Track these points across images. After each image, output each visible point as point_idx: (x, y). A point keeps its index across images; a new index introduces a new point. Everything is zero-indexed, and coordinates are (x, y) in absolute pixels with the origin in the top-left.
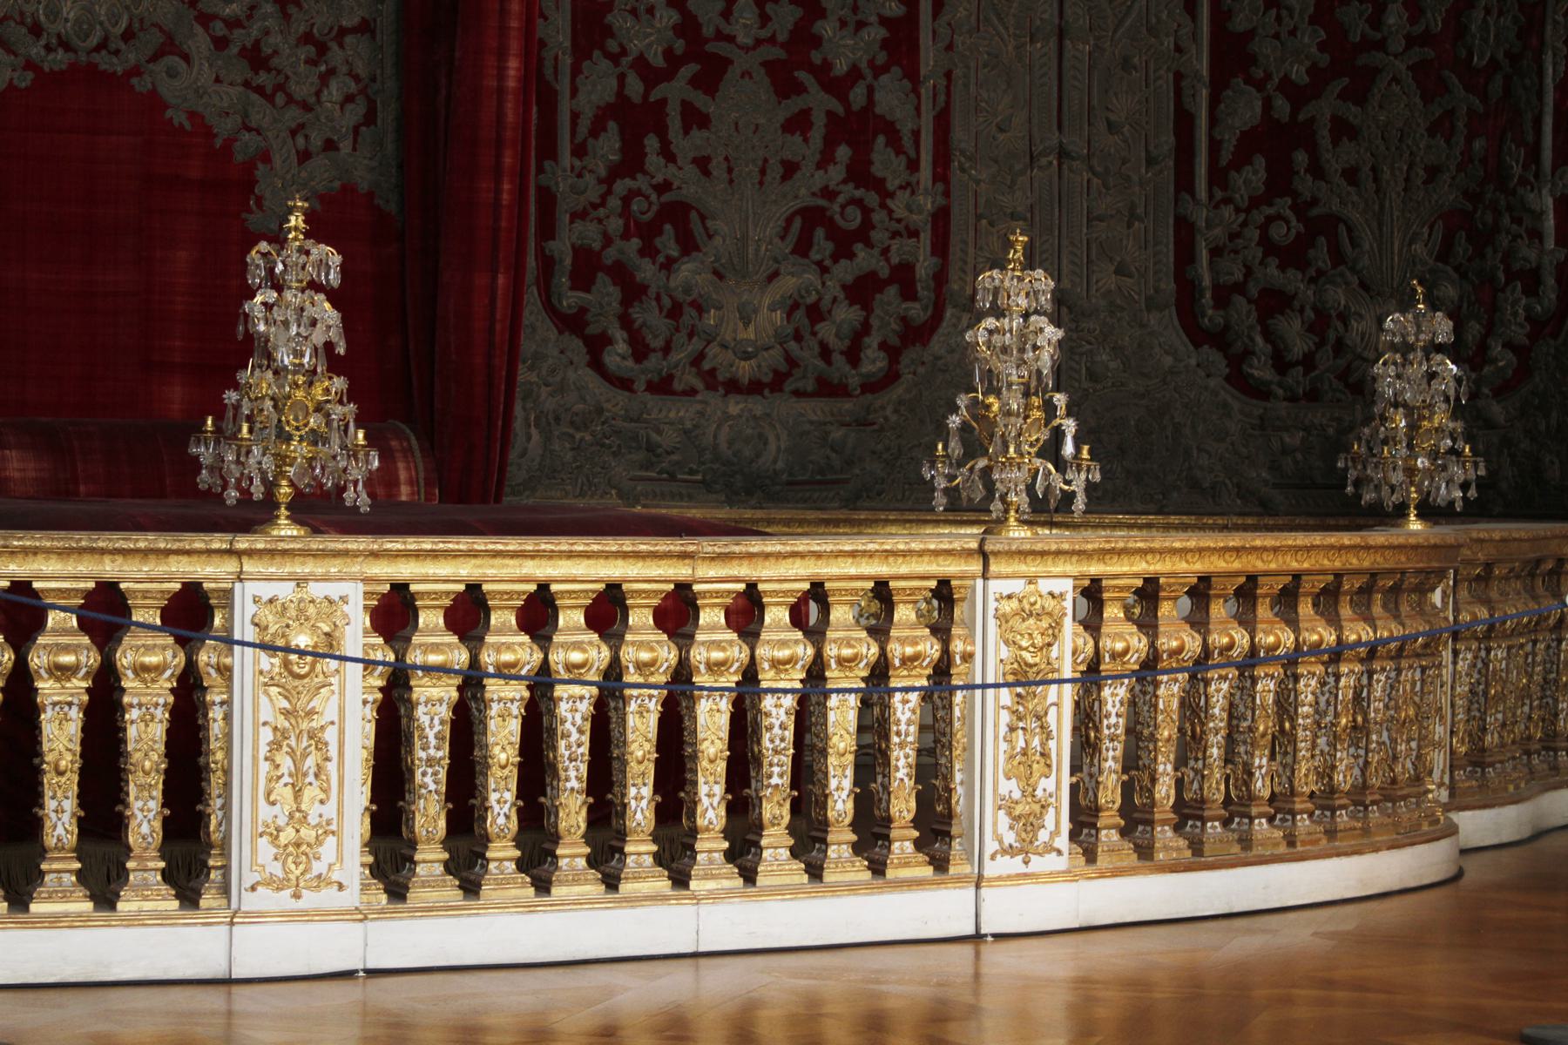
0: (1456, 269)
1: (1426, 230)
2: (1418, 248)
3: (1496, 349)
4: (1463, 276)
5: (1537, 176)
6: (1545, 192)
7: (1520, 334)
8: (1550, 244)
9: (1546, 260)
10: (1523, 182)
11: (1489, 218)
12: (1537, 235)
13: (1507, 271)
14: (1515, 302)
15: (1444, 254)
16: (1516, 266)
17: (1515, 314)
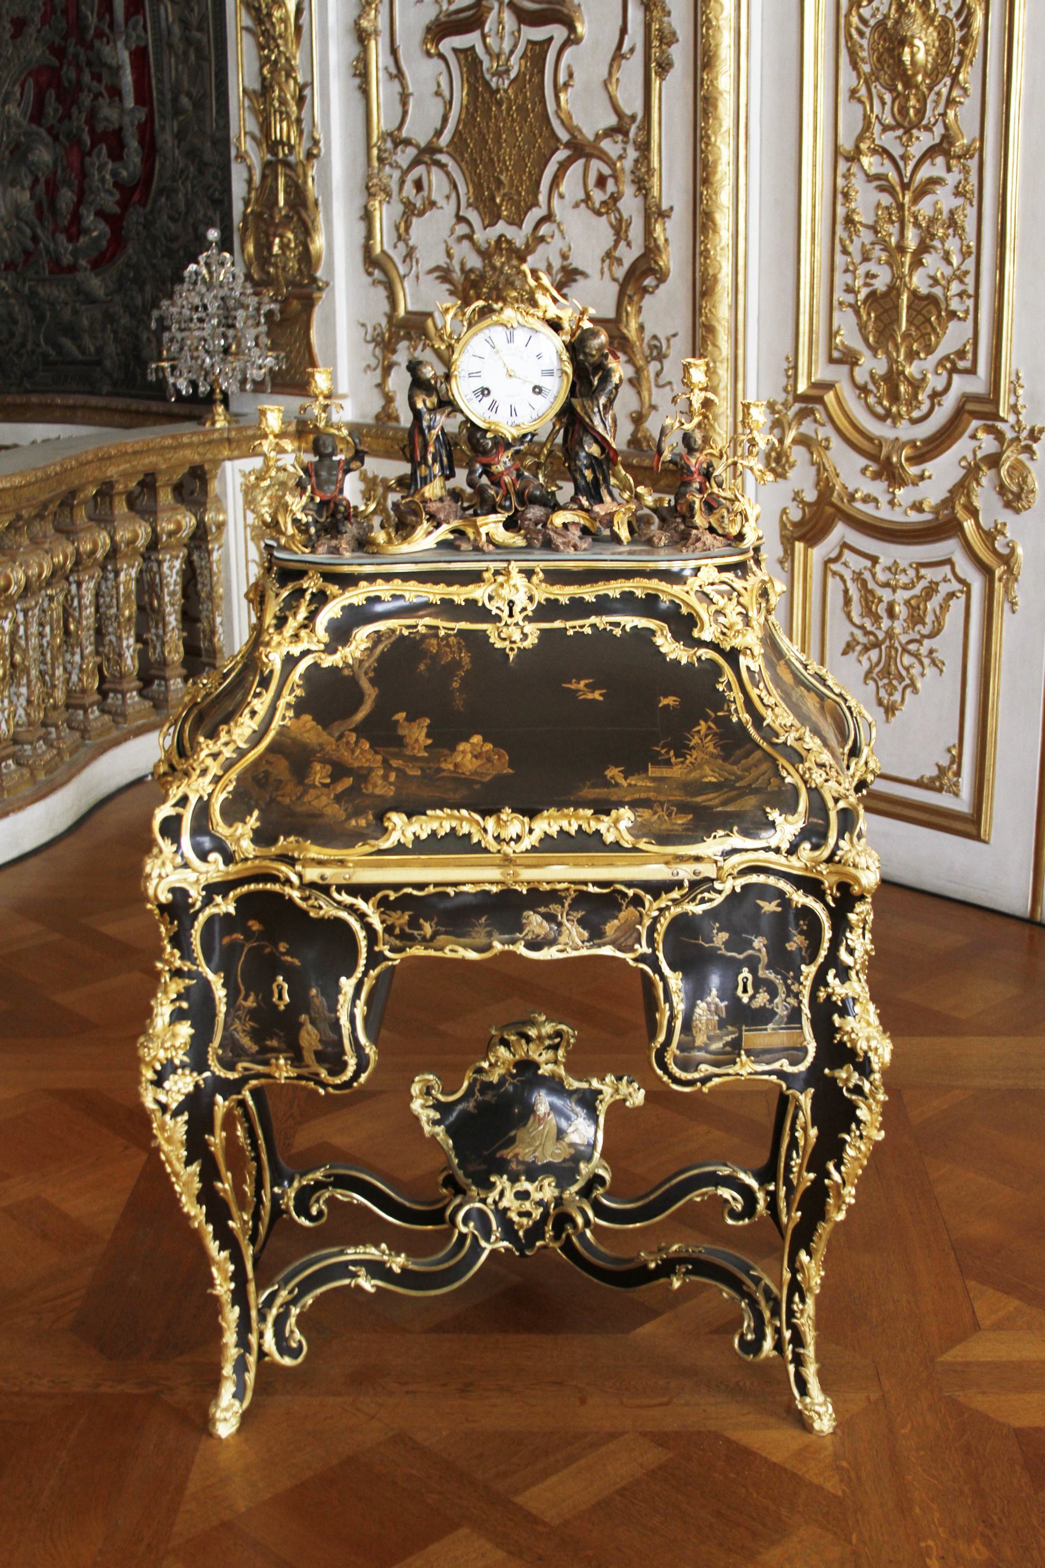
0: (50, 130)
1: (17, 89)
2: (12, 109)
3: (89, 219)
4: (56, 138)
5: (111, 25)
6: (120, 44)
7: (110, 202)
8: (130, 102)
9: (127, 120)
10: (99, 34)
11: (73, 75)
12: (115, 92)
13: (92, 132)
14: (102, 167)
15: (37, 116)
16: (100, 128)
17: (103, 180)
